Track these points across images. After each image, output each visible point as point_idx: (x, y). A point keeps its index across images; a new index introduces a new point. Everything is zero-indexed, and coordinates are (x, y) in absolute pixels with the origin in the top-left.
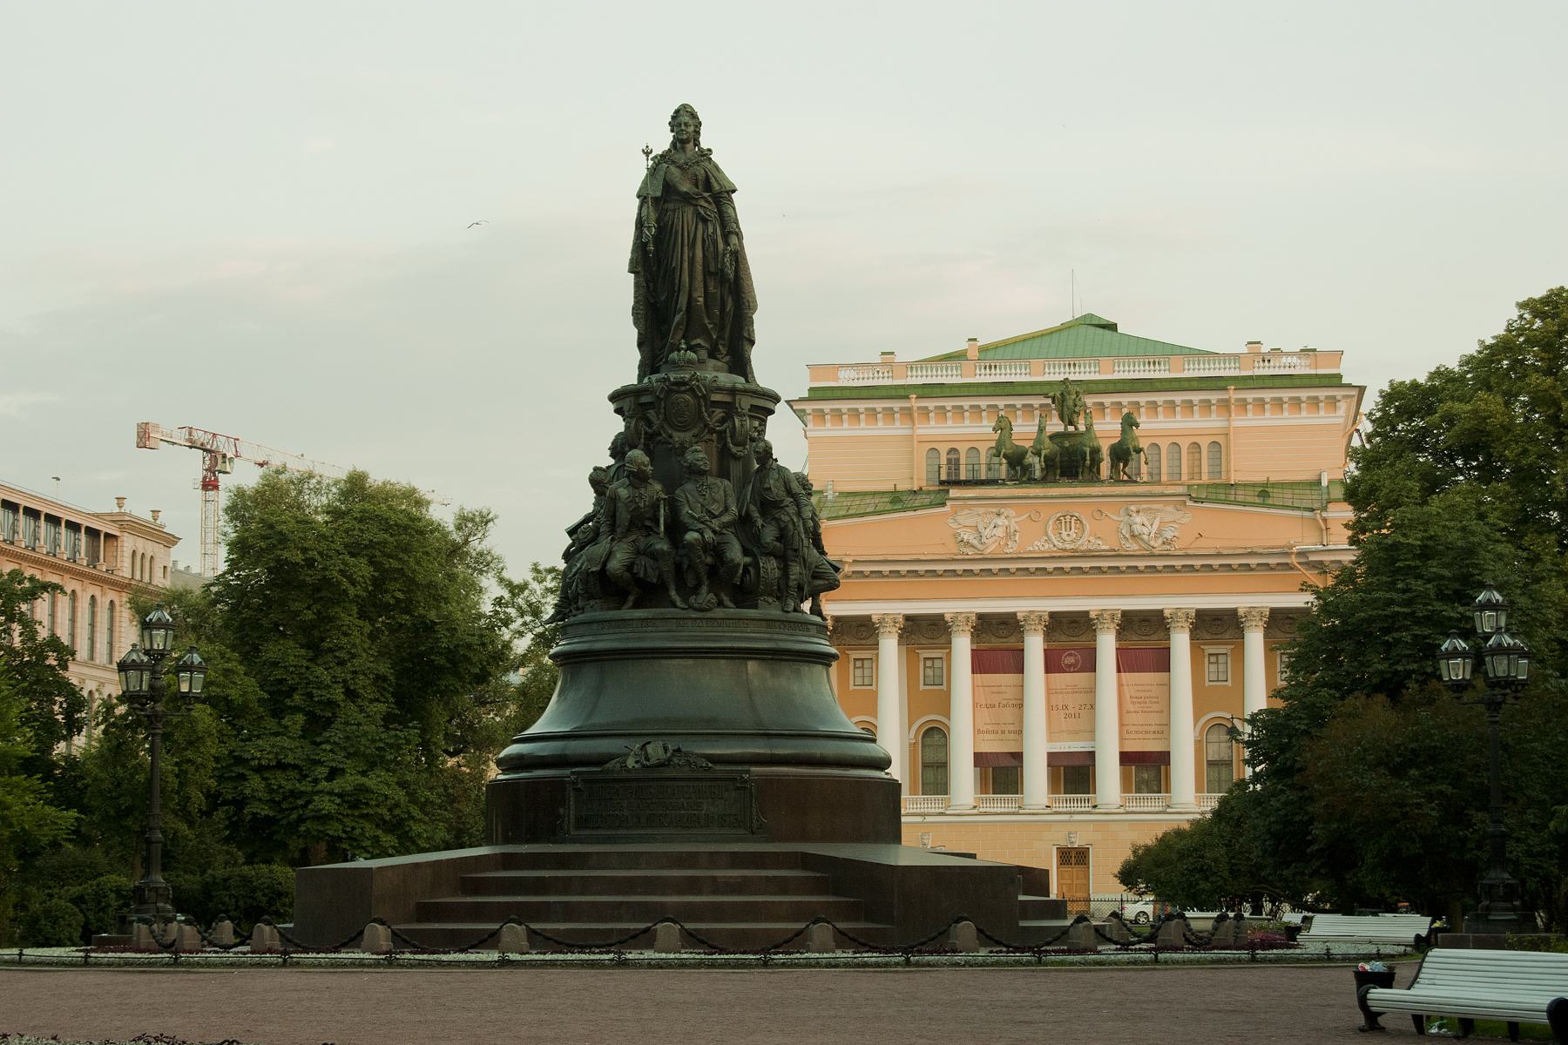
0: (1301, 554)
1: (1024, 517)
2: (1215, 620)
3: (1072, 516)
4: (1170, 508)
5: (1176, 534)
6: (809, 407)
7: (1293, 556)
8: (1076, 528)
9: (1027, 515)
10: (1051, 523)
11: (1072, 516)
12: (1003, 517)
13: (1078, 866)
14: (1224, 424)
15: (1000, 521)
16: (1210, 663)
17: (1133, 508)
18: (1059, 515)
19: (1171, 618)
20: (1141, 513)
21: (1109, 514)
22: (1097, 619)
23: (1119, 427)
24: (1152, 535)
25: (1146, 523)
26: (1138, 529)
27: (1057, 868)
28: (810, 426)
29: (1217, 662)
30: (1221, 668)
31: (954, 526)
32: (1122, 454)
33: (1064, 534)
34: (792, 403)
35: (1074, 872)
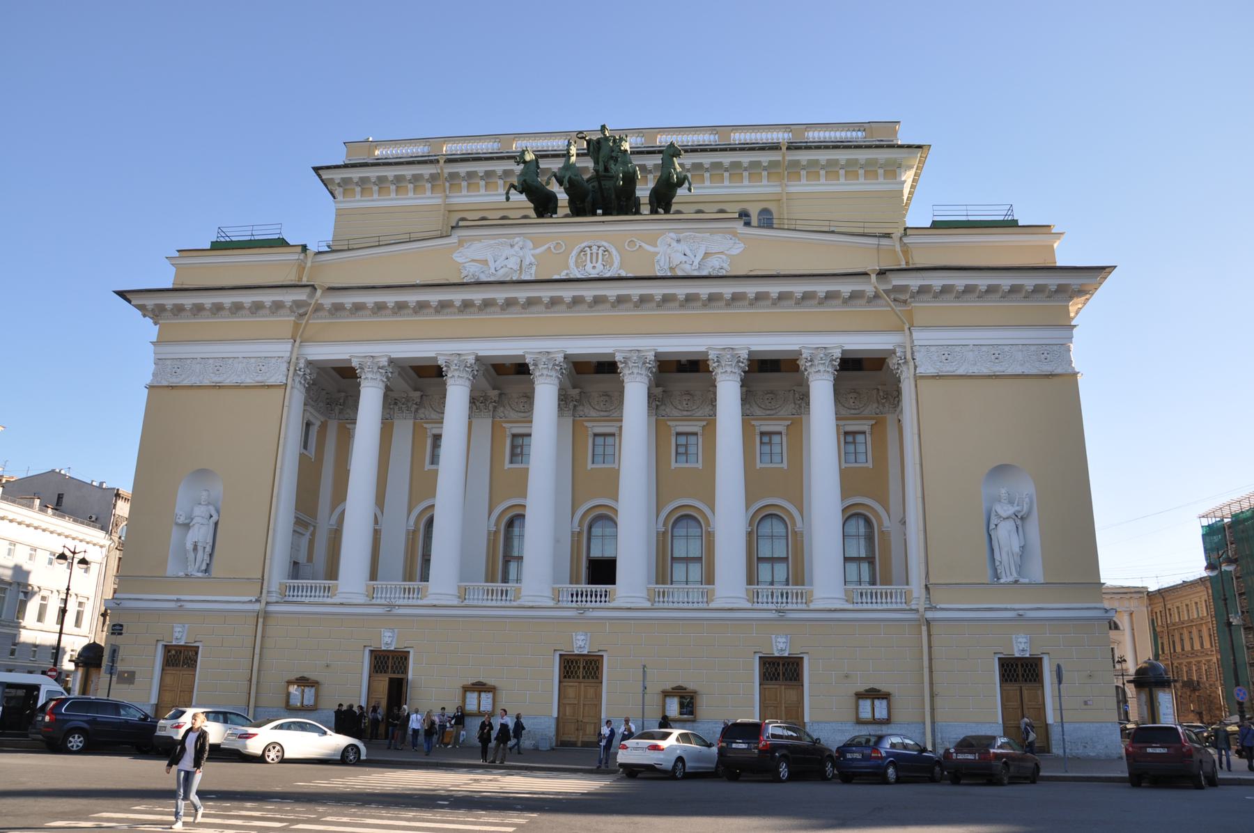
0: (882, 273)
1: (546, 246)
2: (768, 393)
3: (599, 247)
4: (717, 237)
5: (725, 266)
6: (337, 175)
7: (873, 277)
8: (603, 260)
9: (546, 246)
10: (574, 253)
11: (599, 247)
12: (516, 248)
13: (586, 680)
14: (778, 190)
15: (512, 251)
16: (761, 443)
17: (672, 235)
18: (583, 245)
19: (718, 361)
20: (682, 242)
21: (643, 244)
22: (625, 362)
23: (661, 162)
24: (696, 263)
25: (688, 253)
26: (677, 258)
27: (560, 682)
28: (340, 198)
29: (770, 443)
30: (776, 449)
31: (459, 260)
32: (663, 199)
33: (589, 266)
34: (321, 172)
35: (582, 688)
